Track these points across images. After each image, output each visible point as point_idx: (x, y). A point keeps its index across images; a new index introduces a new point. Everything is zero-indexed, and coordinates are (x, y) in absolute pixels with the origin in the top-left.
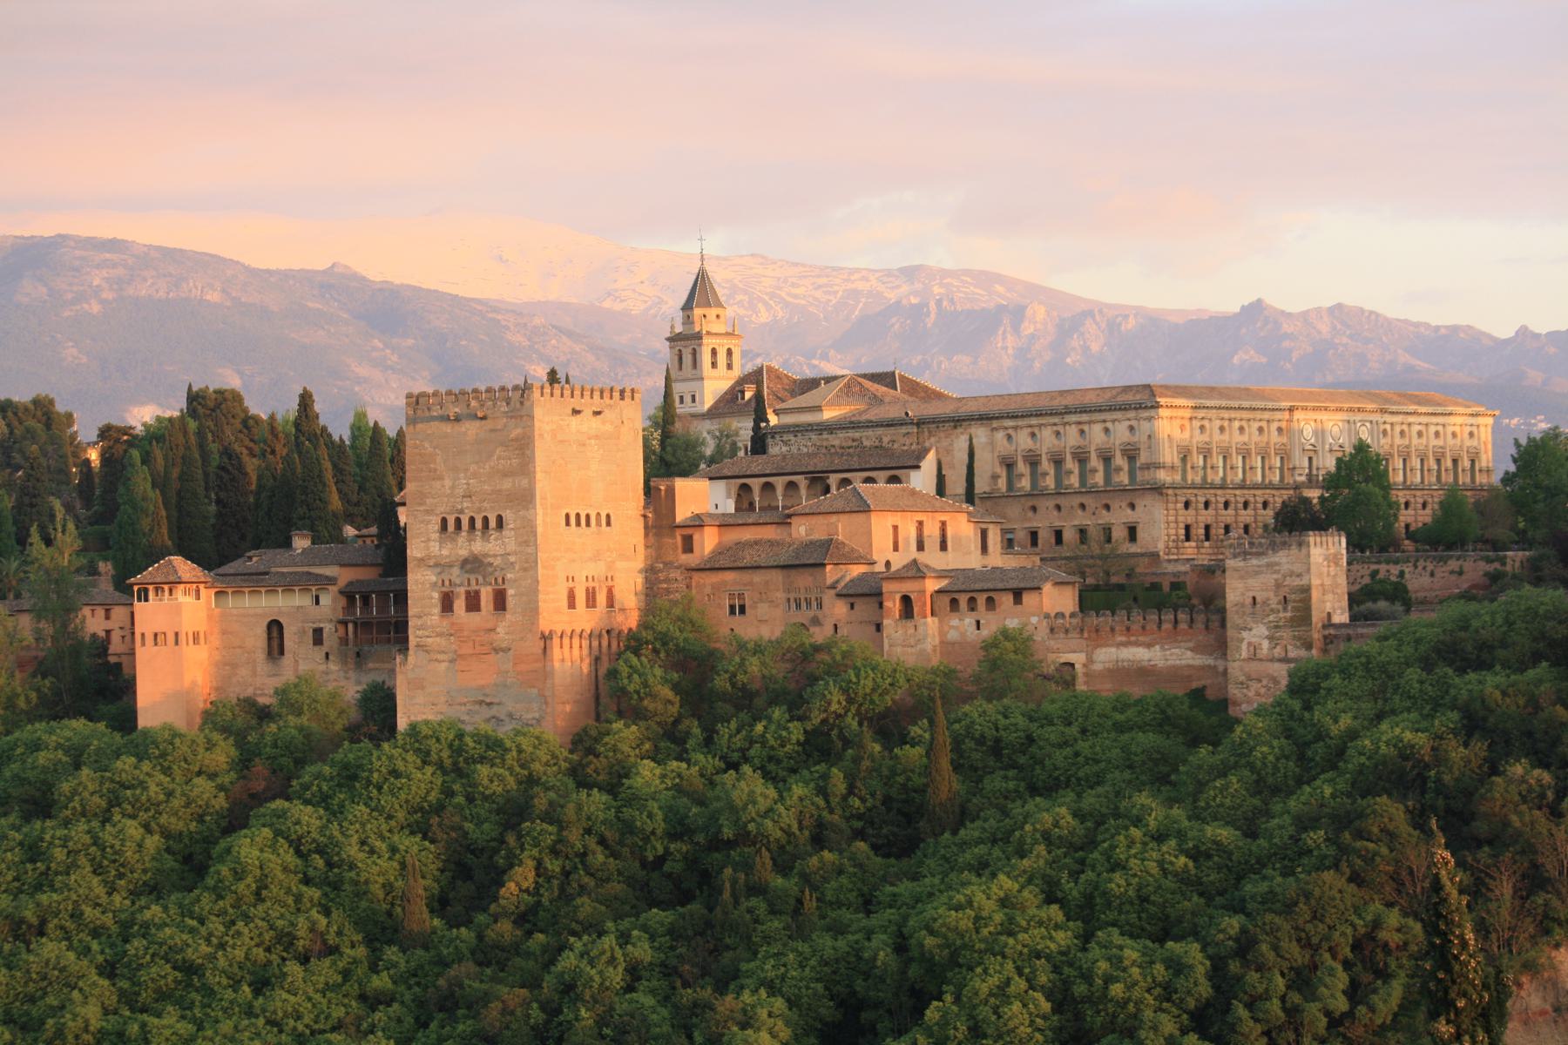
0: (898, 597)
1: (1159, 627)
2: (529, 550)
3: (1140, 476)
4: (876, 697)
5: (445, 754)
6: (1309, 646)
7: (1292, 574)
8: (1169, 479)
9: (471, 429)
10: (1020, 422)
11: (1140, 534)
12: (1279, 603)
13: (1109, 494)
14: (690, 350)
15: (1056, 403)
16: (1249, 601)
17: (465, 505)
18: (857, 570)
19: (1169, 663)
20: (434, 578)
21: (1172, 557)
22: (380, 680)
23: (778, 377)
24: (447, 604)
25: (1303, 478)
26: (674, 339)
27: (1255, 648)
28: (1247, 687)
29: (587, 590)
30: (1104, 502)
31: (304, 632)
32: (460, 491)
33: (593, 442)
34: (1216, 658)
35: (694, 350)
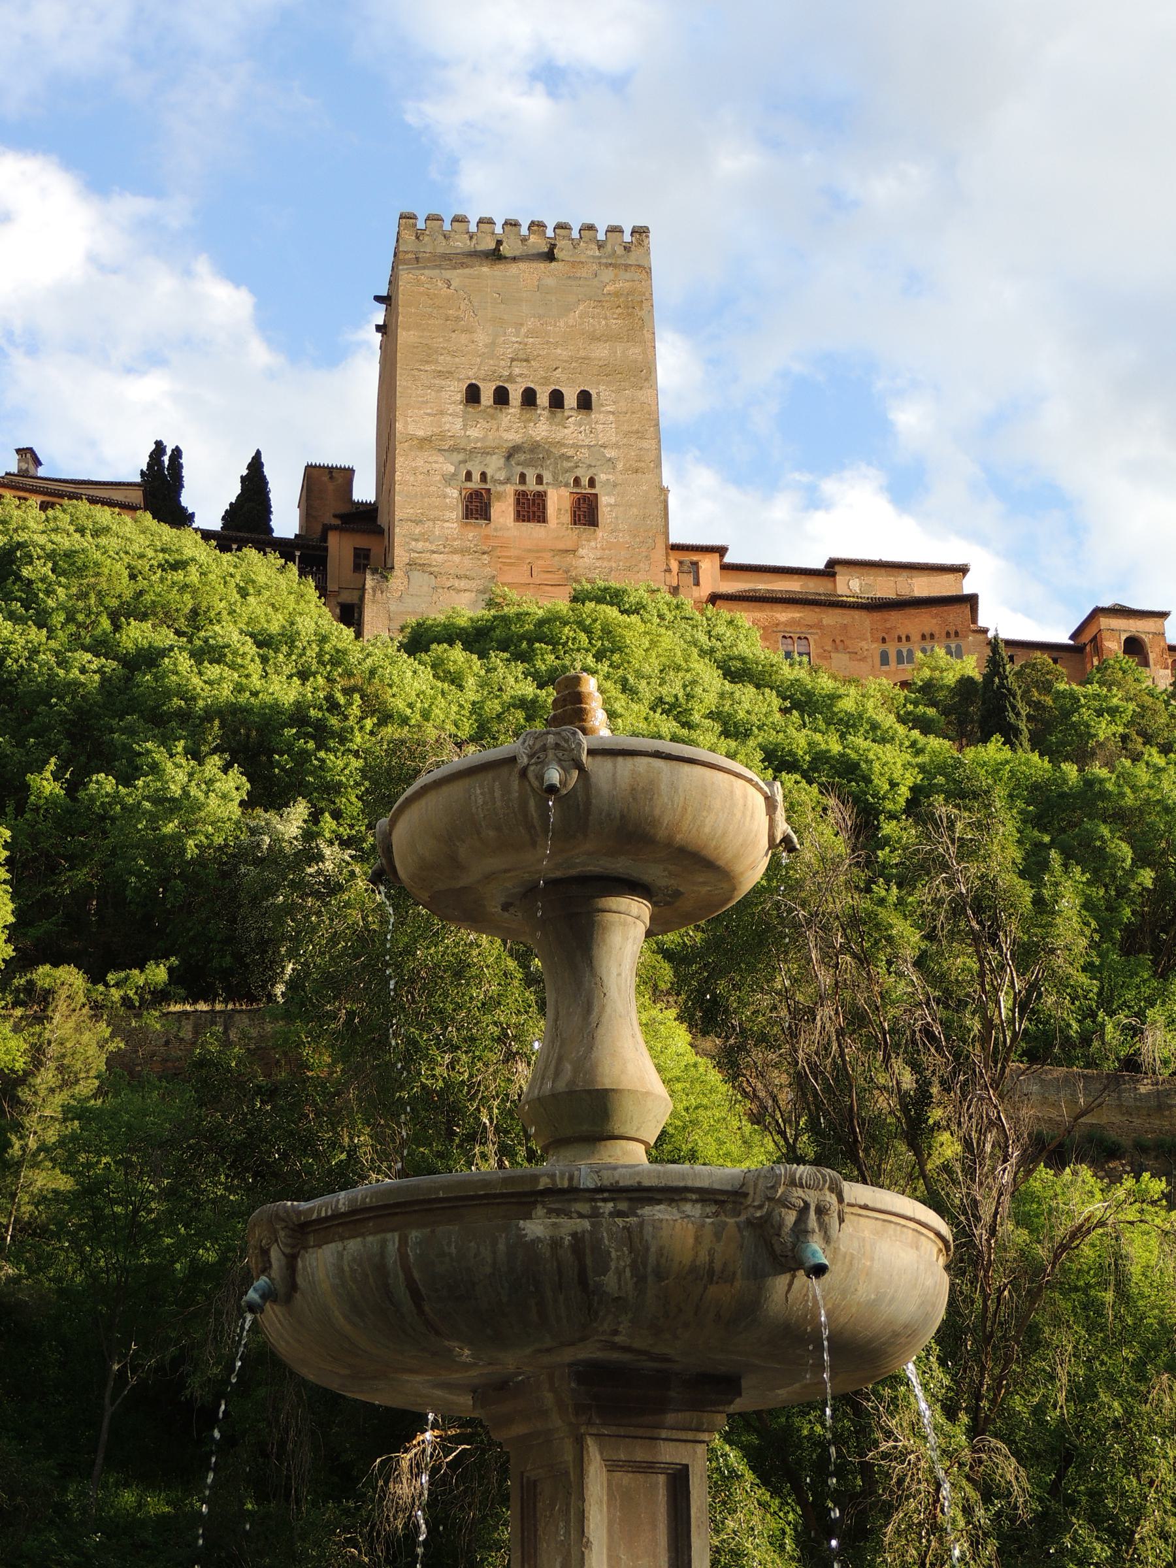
0: (1123, 638)
2: (645, 444)
9: (528, 274)
17: (517, 371)
20: (452, 469)
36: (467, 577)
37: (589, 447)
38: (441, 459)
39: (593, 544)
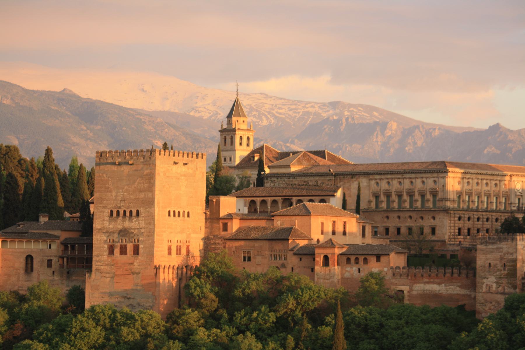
0: (322, 256)
1: (444, 275)
2: (151, 227)
3: (438, 204)
4: (310, 303)
5: (107, 321)
6: (515, 287)
7: (508, 253)
8: (451, 206)
9: (125, 169)
10: (383, 177)
11: (437, 231)
12: (502, 266)
13: (423, 211)
14: (230, 136)
15: (400, 168)
16: (487, 265)
17: (122, 204)
18: (302, 243)
19: (449, 292)
20: (105, 238)
21: (451, 243)
22: (78, 285)
23: (270, 151)
24: (111, 251)
25: (515, 208)
26: (222, 131)
27: (489, 287)
28: (485, 306)
29: (177, 247)
30: (420, 216)
31: (43, 261)
32: (120, 198)
33: (183, 177)
34: (471, 291)
35: (232, 136)
36: (108, 273)
37: (138, 229)
38: (103, 236)
39: (137, 261)
